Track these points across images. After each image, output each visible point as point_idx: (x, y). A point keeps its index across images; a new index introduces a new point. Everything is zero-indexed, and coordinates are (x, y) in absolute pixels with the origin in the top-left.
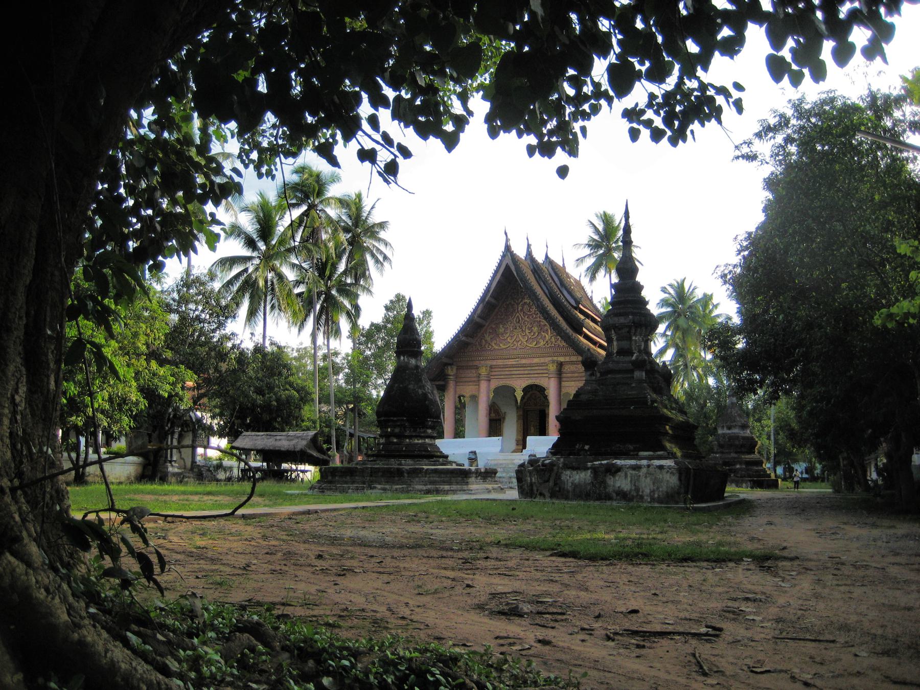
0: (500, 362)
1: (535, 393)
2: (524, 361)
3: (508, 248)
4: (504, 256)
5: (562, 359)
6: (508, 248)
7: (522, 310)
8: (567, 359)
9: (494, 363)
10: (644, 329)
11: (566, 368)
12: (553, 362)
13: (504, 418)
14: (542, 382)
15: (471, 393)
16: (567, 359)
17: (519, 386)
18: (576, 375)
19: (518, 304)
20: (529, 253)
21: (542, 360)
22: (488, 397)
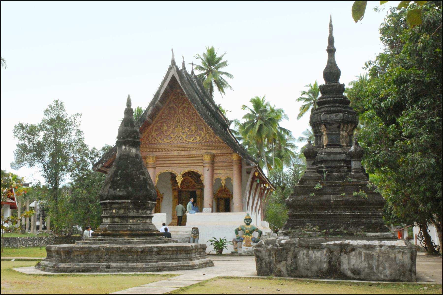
0: (164, 154)
1: (194, 178)
2: (183, 153)
3: (173, 63)
4: (170, 68)
5: (214, 152)
6: (173, 63)
7: (182, 112)
8: (219, 152)
9: (159, 154)
10: (349, 125)
11: (218, 159)
12: (208, 154)
13: (162, 198)
14: (199, 170)
16: (219, 152)
17: (179, 173)
19: (179, 107)
20: (184, 68)
21: (199, 152)
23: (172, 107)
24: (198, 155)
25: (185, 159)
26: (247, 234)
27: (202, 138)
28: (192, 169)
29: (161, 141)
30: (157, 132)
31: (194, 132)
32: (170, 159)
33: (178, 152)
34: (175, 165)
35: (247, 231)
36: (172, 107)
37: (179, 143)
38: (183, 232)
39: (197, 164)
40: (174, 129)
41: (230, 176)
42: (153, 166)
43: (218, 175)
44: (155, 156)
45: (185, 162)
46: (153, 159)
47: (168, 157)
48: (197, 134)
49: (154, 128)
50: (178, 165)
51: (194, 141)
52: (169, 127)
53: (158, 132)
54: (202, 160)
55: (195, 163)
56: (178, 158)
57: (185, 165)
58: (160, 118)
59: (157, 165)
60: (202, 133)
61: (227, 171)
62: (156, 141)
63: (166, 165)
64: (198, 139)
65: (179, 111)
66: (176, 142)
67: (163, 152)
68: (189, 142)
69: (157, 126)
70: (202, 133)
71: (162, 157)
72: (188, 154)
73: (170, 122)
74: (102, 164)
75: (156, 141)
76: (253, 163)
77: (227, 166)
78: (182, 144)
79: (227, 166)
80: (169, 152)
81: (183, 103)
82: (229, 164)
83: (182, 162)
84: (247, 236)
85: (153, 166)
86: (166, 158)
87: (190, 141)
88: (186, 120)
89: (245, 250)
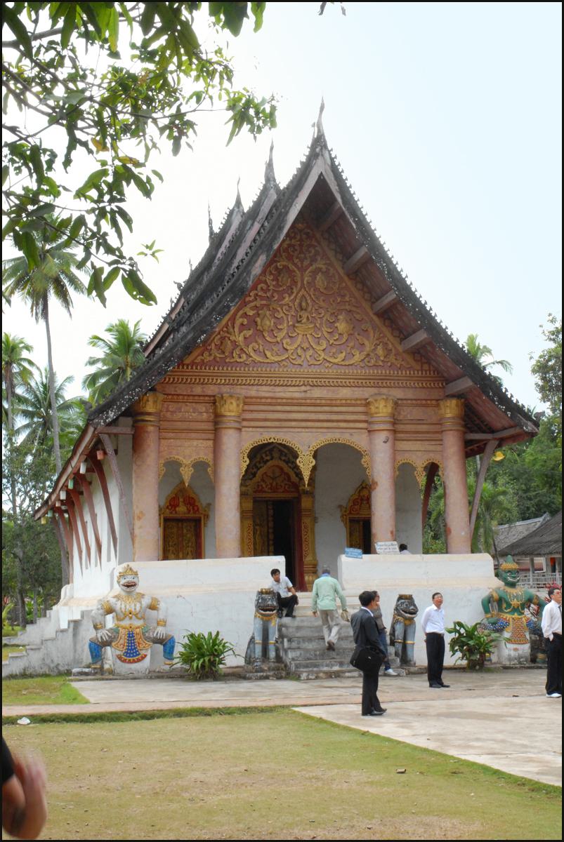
0: (264, 392)
2: (317, 393)
9: (253, 392)
14: (358, 440)
15: (195, 457)
18: (424, 428)
19: (303, 270)
22: (240, 469)
23: (285, 267)
24: (357, 400)
25: (319, 409)
26: (515, 610)
27: (368, 355)
29: (258, 359)
30: (249, 333)
31: (345, 337)
32: (279, 408)
33: (303, 388)
34: (293, 424)
35: (515, 602)
36: (285, 267)
37: (305, 364)
39: (352, 425)
40: (294, 326)
41: (436, 458)
42: (236, 425)
43: (407, 455)
44: (242, 397)
45: (322, 417)
46: (238, 405)
47: (274, 402)
48: (352, 344)
49: (239, 321)
50: (304, 424)
51: (343, 363)
52: (279, 321)
53: (250, 332)
54: (366, 413)
56: (301, 405)
59: (245, 423)
60: (367, 343)
61: (426, 446)
62: (244, 356)
64: (358, 357)
65: (302, 281)
66: (299, 362)
67: (265, 388)
68: (334, 364)
69: (245, 315)
70: (367, 343)
71: (258, 400)
72: (330, 395)
73: (281, 306)
74: (119, 408)
75: (244, 356)
76: (529, 423)
77: (428, 432)
78: (313, 369)
79: (428, 432)
80: (278, 389)
81: (313, 260)
82: (432, 428)
83: (313, 416)
84: (516, 615)
85: (236, 425)
86: (270, 404)
87: (336, 361)
88: (322, 304)
89: (513, 654)
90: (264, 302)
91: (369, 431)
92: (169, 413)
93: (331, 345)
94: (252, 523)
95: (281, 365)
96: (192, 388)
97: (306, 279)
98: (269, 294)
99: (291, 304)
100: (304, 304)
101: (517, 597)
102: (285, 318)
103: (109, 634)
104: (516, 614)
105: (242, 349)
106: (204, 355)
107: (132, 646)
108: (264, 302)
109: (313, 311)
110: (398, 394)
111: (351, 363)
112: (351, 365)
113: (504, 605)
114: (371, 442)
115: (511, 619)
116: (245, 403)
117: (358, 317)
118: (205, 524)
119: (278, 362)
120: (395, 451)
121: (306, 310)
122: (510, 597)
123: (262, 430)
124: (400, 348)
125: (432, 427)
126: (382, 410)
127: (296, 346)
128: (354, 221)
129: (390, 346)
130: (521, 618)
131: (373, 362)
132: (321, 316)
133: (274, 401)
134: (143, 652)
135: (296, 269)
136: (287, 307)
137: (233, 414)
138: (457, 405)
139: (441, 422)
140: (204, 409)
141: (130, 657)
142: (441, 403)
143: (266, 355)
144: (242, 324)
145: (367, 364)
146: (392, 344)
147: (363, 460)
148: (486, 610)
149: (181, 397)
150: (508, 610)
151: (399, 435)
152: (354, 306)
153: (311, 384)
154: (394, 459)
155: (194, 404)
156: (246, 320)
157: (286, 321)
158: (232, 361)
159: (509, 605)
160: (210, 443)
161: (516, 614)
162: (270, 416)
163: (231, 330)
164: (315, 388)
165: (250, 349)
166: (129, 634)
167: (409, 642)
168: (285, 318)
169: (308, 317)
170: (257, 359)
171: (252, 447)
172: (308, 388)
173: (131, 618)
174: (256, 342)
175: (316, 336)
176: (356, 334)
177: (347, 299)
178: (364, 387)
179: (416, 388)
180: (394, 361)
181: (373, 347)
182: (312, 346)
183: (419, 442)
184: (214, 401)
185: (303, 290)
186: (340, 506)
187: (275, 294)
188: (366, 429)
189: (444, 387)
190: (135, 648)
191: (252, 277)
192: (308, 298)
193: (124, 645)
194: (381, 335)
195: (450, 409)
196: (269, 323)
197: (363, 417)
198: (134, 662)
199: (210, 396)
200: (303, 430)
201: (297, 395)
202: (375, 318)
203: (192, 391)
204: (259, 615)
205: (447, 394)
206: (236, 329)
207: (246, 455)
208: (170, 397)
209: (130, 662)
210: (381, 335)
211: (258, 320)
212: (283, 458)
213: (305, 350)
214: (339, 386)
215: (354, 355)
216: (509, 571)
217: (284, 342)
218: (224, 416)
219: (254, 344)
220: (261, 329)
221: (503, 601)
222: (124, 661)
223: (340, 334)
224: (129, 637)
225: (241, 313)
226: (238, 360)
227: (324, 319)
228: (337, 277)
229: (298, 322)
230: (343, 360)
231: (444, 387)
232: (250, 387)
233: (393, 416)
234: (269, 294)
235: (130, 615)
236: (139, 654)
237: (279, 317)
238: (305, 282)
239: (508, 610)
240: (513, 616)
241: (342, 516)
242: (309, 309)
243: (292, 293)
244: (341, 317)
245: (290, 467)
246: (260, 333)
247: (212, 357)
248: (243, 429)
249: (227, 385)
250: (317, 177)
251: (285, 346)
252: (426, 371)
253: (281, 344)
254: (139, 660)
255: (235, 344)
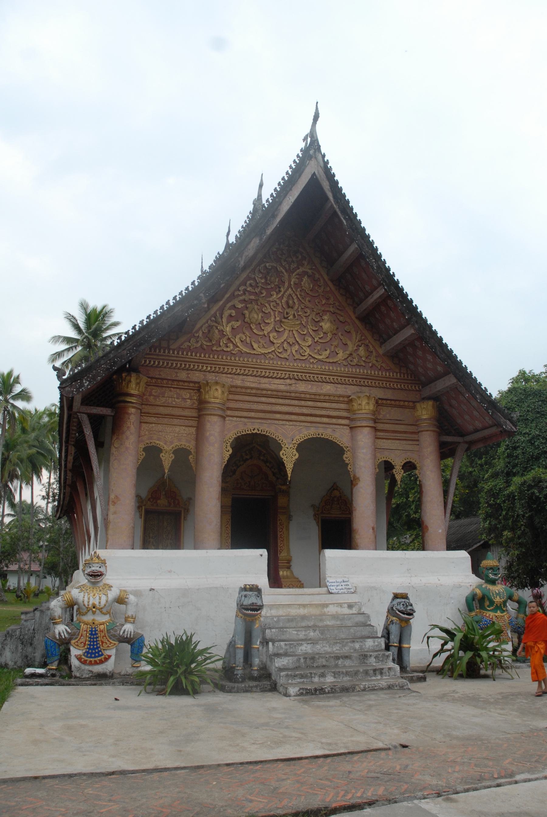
0: (250, 382)
2: (302, 387)
9: (238, 381)
14: (340, 435)
15: (176, 444)
19: (290, 272)
21: (341, 390)
22: (223, 458)
24: (340, 396)
25: (303, 403)
27: (351, 354)
28: (321, 431)
30: (237, 324)
31: (329, 336)
32: (264, 399)
33: (288, 381)
34: (278, 416)
38: (340, 605)
39: (334, 421)
40: (281, 321)
41: (413, 457)
45: (305, 411)
46: (223, 393)
47: (260, 393)
48: (335, 343)
50: (287, 417)
51: (328, 360)
52: (267, 315)
53: (238, 324)
54: (348, 410)
55: (328, 417)
57: (302, 418)
58: (242, 288)
59: (229, 413)
60: (349, 343)
62: (231, 345)
63: (252, 414)
64: (341, 355)
66: (285, 355)
67: (251, 379)
68: (319, 360)
69: (234, 307)
70: (349, 343)
77: (405, 432)
79: (405, 432)
83: (297, 410)
84: (499, 613)
85: (220, 412)
86: (255, 395)
88: (308, 304)
90: (253, 297)
91: (351, 428)
92: (152, 397)
93: (315, 342)
94: (230, 518)
95: (267, 357)
96: (177, 373)
97: (293, 280)
98: (257, 290)
99: (278, 302)
100: (291, 302)
101: (499, 594)
102: (272, 313)
103: (69, 630)
104: (499, 612)
105: (229, 339)
106: (191, 342)
107: (94, 645)
108: (253, 297)
109: (299, 309)
110: (379, 393)
111: (335, 361)
112: (335, 363)
113: (487, 603)
114: (353, 438)
115: (494, 618)
116: (230, 392)
117: (341, 319)
118: (184, 517)
119: (264, 354)
120: (376, 449)
121: (292, 308)
122: (493, 594)
123: (246, 420)
124: (381, 351)
125: (409, 427)
126: (365, 406)
127: (283, 341)
128: (345, 218)
129: (371, 348)
130: (504, 616)
131: (355, 361)
132: (307, 315)
133: (259, 392)
134: (108, 653)
135: (283, 271)
136: (274, 303)
137: (217, 401)
138: (433, 407)
139: (417, 423)
140: (188, 396)
141: (91, 657)
142: (418, 405)
143: (252, 346)
144: (230, 316)
145: (350, 362)
146: (373, 347)
147: (345, 456)
148: (470, 609)
149: (165, 381)
150: (491, 608)
151: (379, 433)
152: (338, 309)
153: (296, 378)
154: (375, 457)
155: (178, 390)
156: (234, 312)
157: (273, 317)
158: (218, 349)
159: (492, 602)
160: (193, 430)
161: (499, 612)
162: (255, 407)
163: (220, 320)
164: (300, 382)
165: (237, 340)
166: (92, 631)
167: (405, 646)
168: (272, 313)
169: (294, 315)
170: (244, 350)
171: (235, 436)
172: (293, 381)
173: (94, 613)
174: (244, 333)
175: (302, 333)
176: (340, 334)
177: (331, 301)
178: (347, 384)
179: (395, 389)
180: (375, 362)
181: (355, 348)
182: (298, 342)
183: (397, 442)
184: (199, 388)
185: (290, 290)
186: (313, 506)
187: (264, 291)
188: (348, 425)
189: (420, 391)
190: (98, 648)
191: (244, 257)
192: (295, 297)
193: (85, 644)
194: (363, 338)
195: (425, 412)
196: (257, 316)
197: (345, 414)
198: (96, 663)
199: (195, 383)
200: (287, 423)
201: (282, 387)
202: (357, 322)
203: (177, 376)
204: (241, 615)
205: (423, 397)
206: (224, 320)
207: (229, 444)
208: (154, 381)
209: (91, 663)
210: (363, 338)
211: (246, 312)
212: (262, 458)
213: (291, 345)
214: (324, 382)
215: (337, 354)
216: (491, 568)
217: (271, 335)
218: (209, 402)
219: (241, 335)
220: (249, 322)
221: (486, 599)
222: (84, 663)
223: (324, 333)
224: (91, 634)
225: (229, 305)
226: (225, 349)
227: (310, 317)
228: (322, 281)
229: (285, 318)
230: (327, 358)
231: (420, 391)
232: (236, 377)
233: (374, 413)
234: (257, 290)
235: (94, 609)
236: (102, 655)
237: (267, 312)
238: (292, 283)
239: (491, 608)
240: (496, 614)
241: (315, 515)
242: (296, 308)
243: (280, 291)
244: (325, 317)
245: (268, 467)
246: (248, 325)
247: (199, 345)
248: (227, 419)
249: (213, 372)
250: (310, 176)
251: (272, 339)
252: (404, 374)
253: (268, 338)
254: (101, 662)
255: (221, 332)
